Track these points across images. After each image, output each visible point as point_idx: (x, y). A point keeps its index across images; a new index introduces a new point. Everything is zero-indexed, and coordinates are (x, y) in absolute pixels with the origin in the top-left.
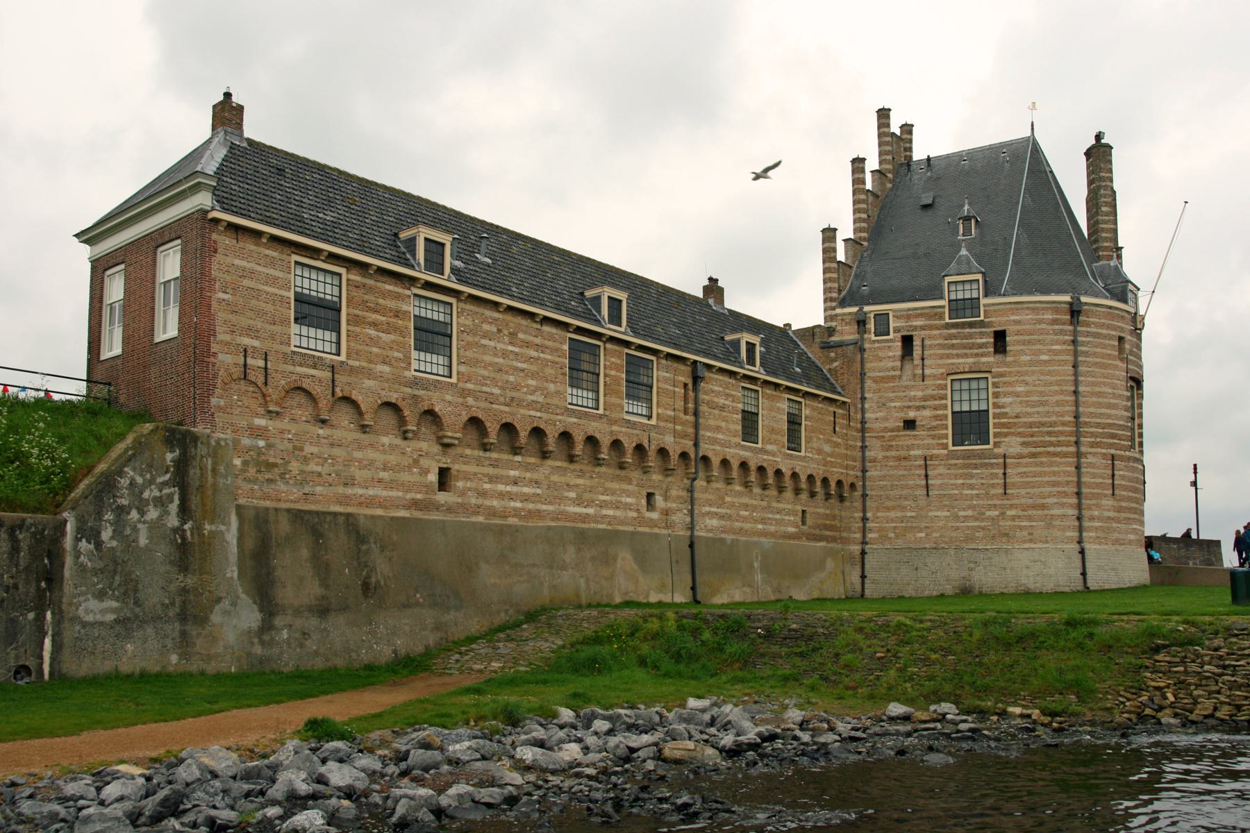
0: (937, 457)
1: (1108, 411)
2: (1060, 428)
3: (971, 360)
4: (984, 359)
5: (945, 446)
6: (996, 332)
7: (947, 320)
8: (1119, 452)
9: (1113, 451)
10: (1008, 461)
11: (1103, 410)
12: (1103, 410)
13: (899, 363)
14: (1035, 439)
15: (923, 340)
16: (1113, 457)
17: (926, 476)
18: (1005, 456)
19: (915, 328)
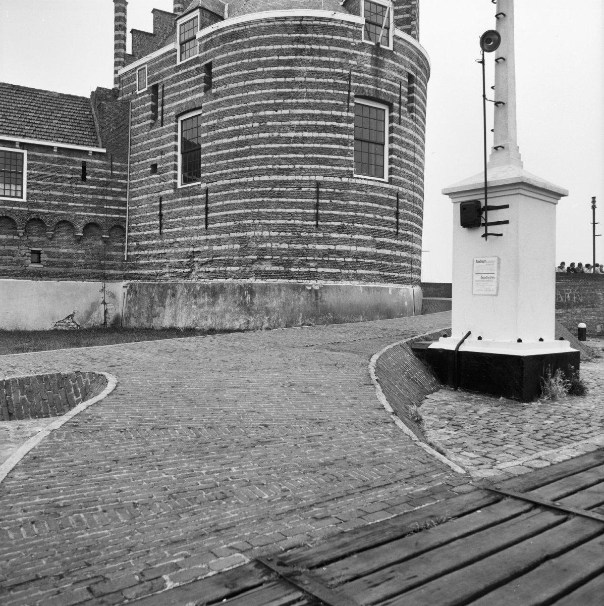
0: (168, 197)
1: (316, 135)
2: (253, 157)
3: (189, 99)
4: (198, 95)
5: (175, 184)
6: (206, 65)
7: (179, 63)
8: (327, 179)
9: (319, 178)
10: (210, 195)
11: (306, 134)
12: (306, 134)
13: (150, 112)
14: (230, 171)
15: (163, 87)
16: (319, 184)
17: (161, 215)
18: (207, 191)
19: (158, 78)
